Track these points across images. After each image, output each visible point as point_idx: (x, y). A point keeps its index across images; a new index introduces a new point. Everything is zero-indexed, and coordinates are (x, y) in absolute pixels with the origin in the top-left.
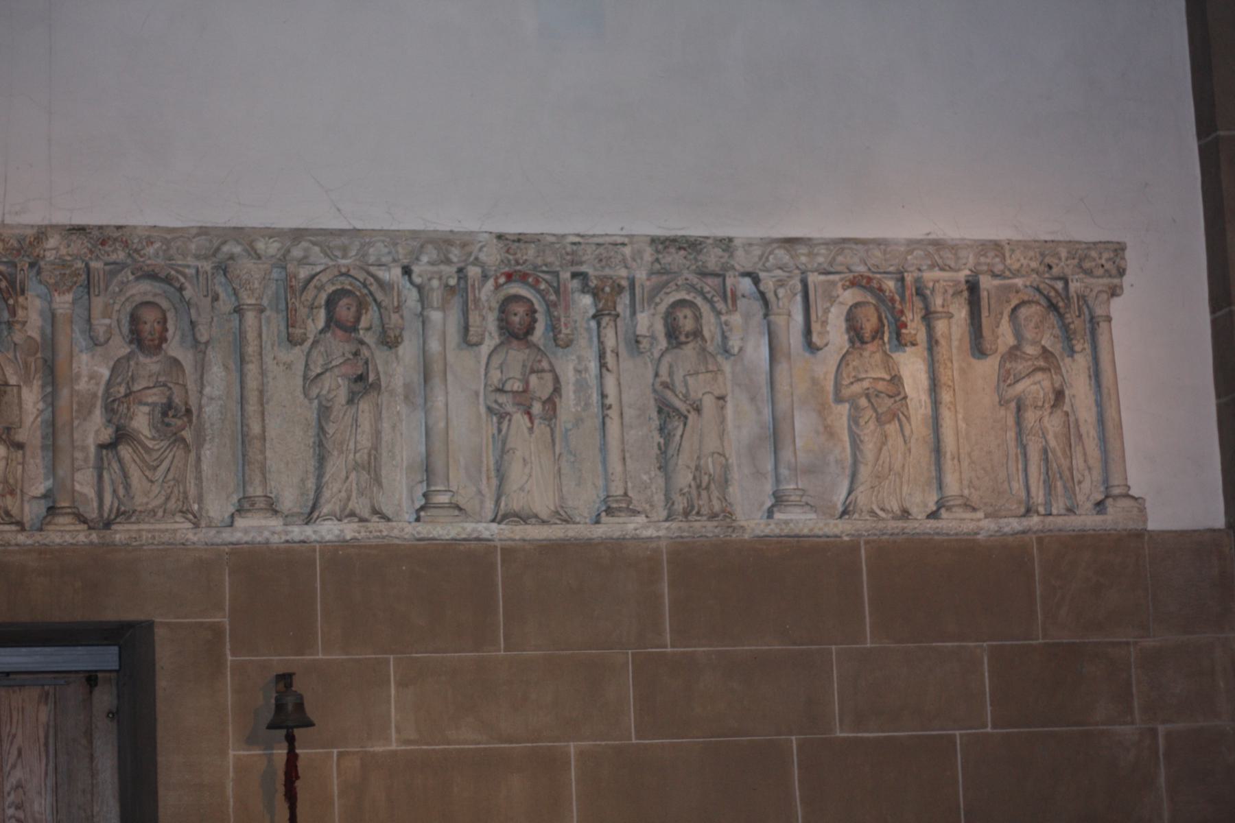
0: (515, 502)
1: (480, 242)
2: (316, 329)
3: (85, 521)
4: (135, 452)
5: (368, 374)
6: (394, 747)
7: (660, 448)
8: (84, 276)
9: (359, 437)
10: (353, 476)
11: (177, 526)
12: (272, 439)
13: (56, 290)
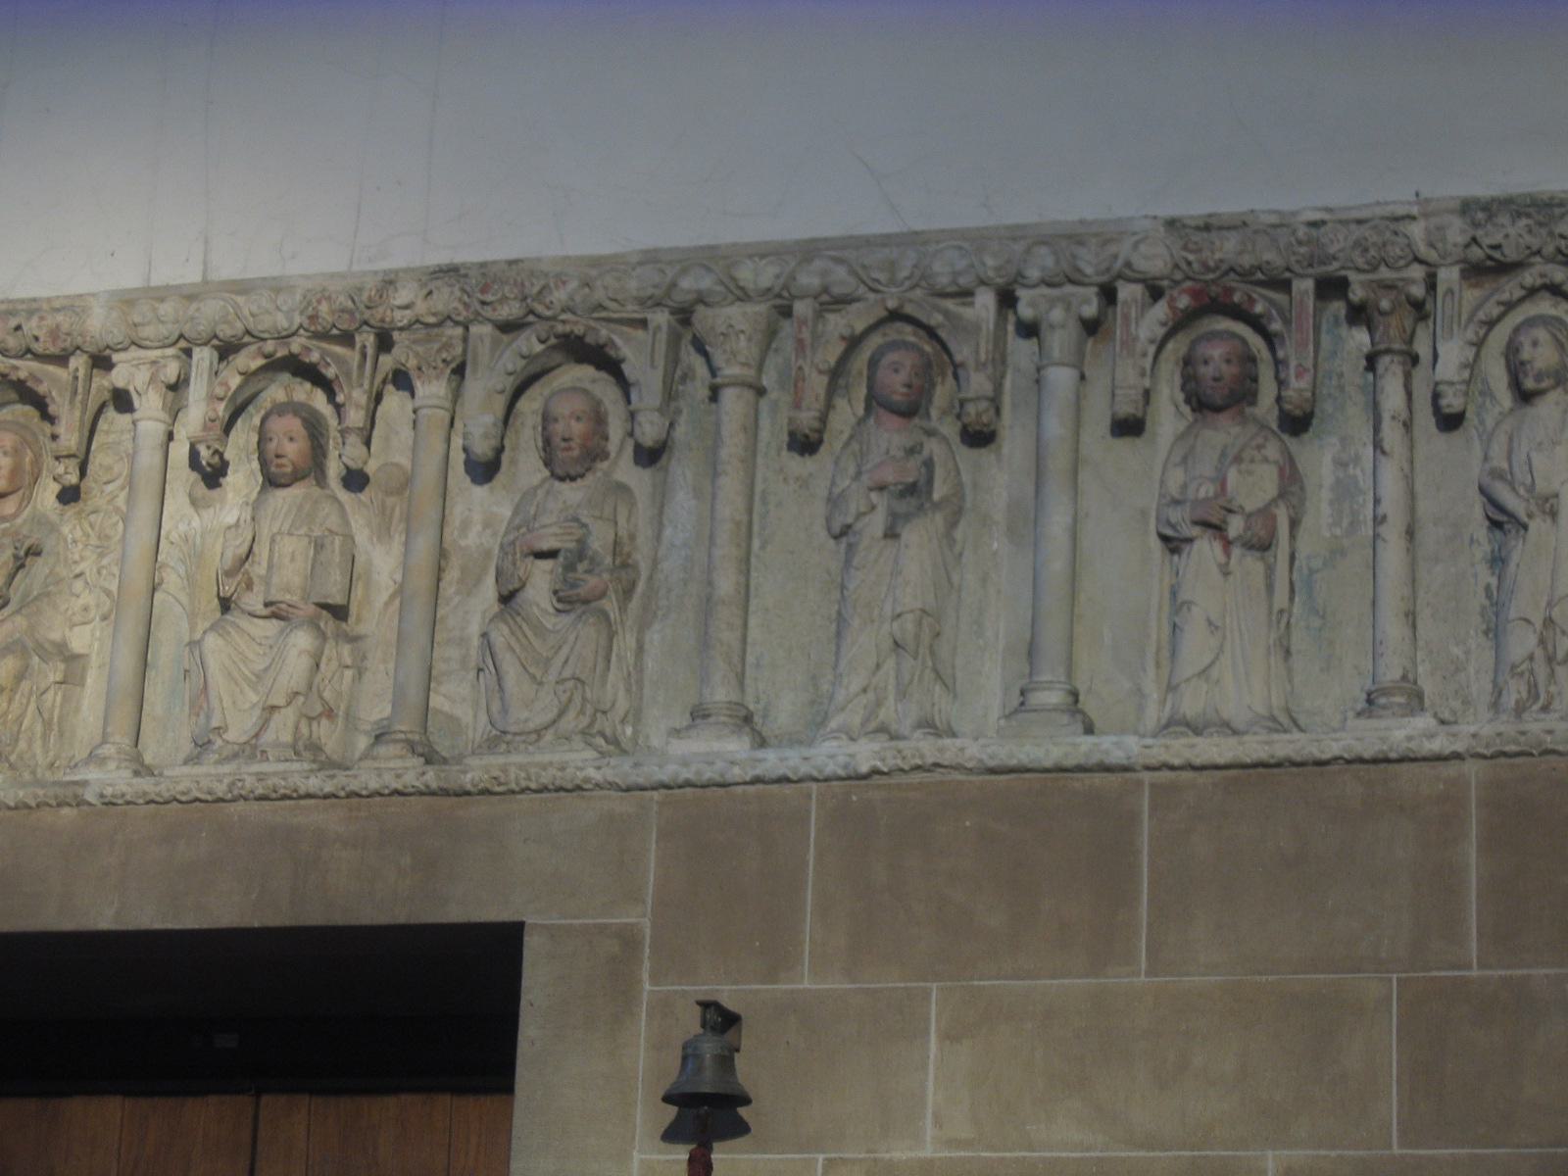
0: (1192, 704)
1: (1134, 234)
4: (513, 633)
6: (927, 1152)
7: (1489, 596)
8: (459, 350)
10: (890, 664)
13: (419, 377)
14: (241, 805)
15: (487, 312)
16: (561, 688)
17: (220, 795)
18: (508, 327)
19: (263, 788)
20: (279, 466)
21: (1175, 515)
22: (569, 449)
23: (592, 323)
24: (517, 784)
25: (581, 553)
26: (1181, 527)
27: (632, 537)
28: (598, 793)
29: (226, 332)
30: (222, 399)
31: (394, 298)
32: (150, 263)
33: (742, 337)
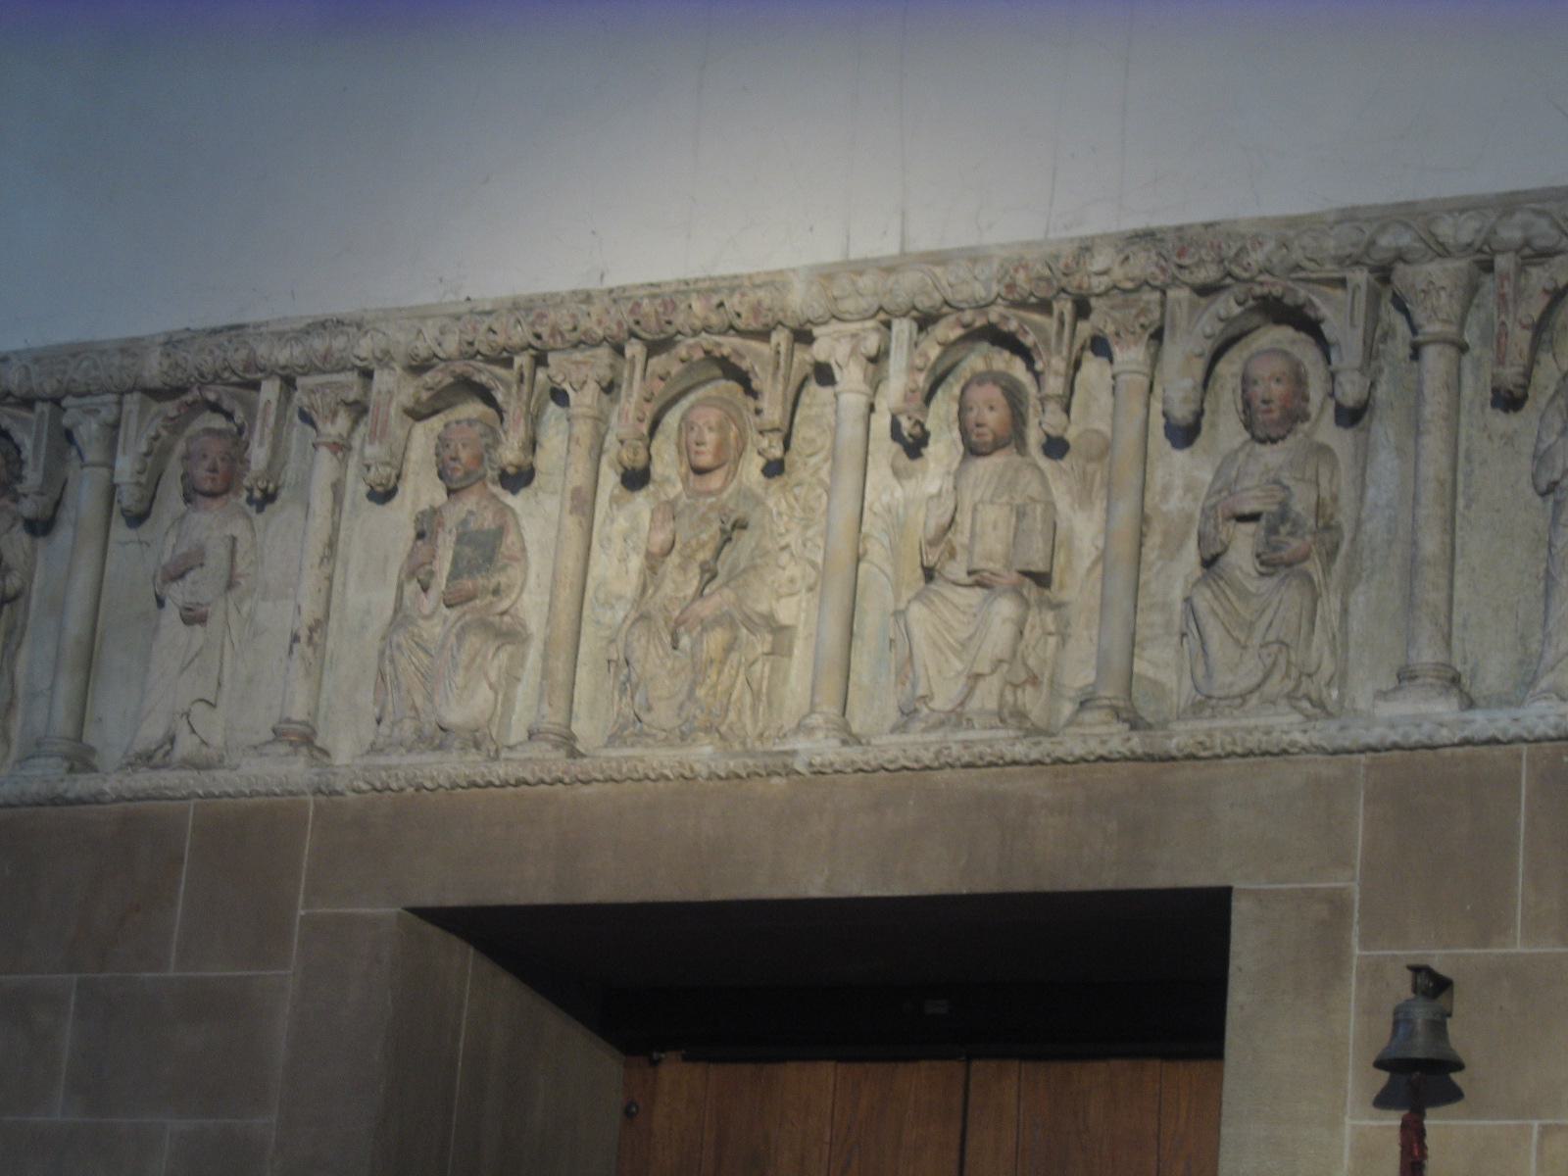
4: (1216, 597)
8: (1157, 314)
13: (1117, 343)
15: (1186, 276)
16: (1265, 651)
17: (927, 763)
18: (1206, 291)
20: (978, 435)
22: (1269, 411)
23: (1290, 284)
25: (1283, 515)
27: (1335, 499)
28: (1304, 757)
29: (924, 303)
30: (920, 370)
31: (1091, 265)
32: (848, 238)
33: (1443, 294)
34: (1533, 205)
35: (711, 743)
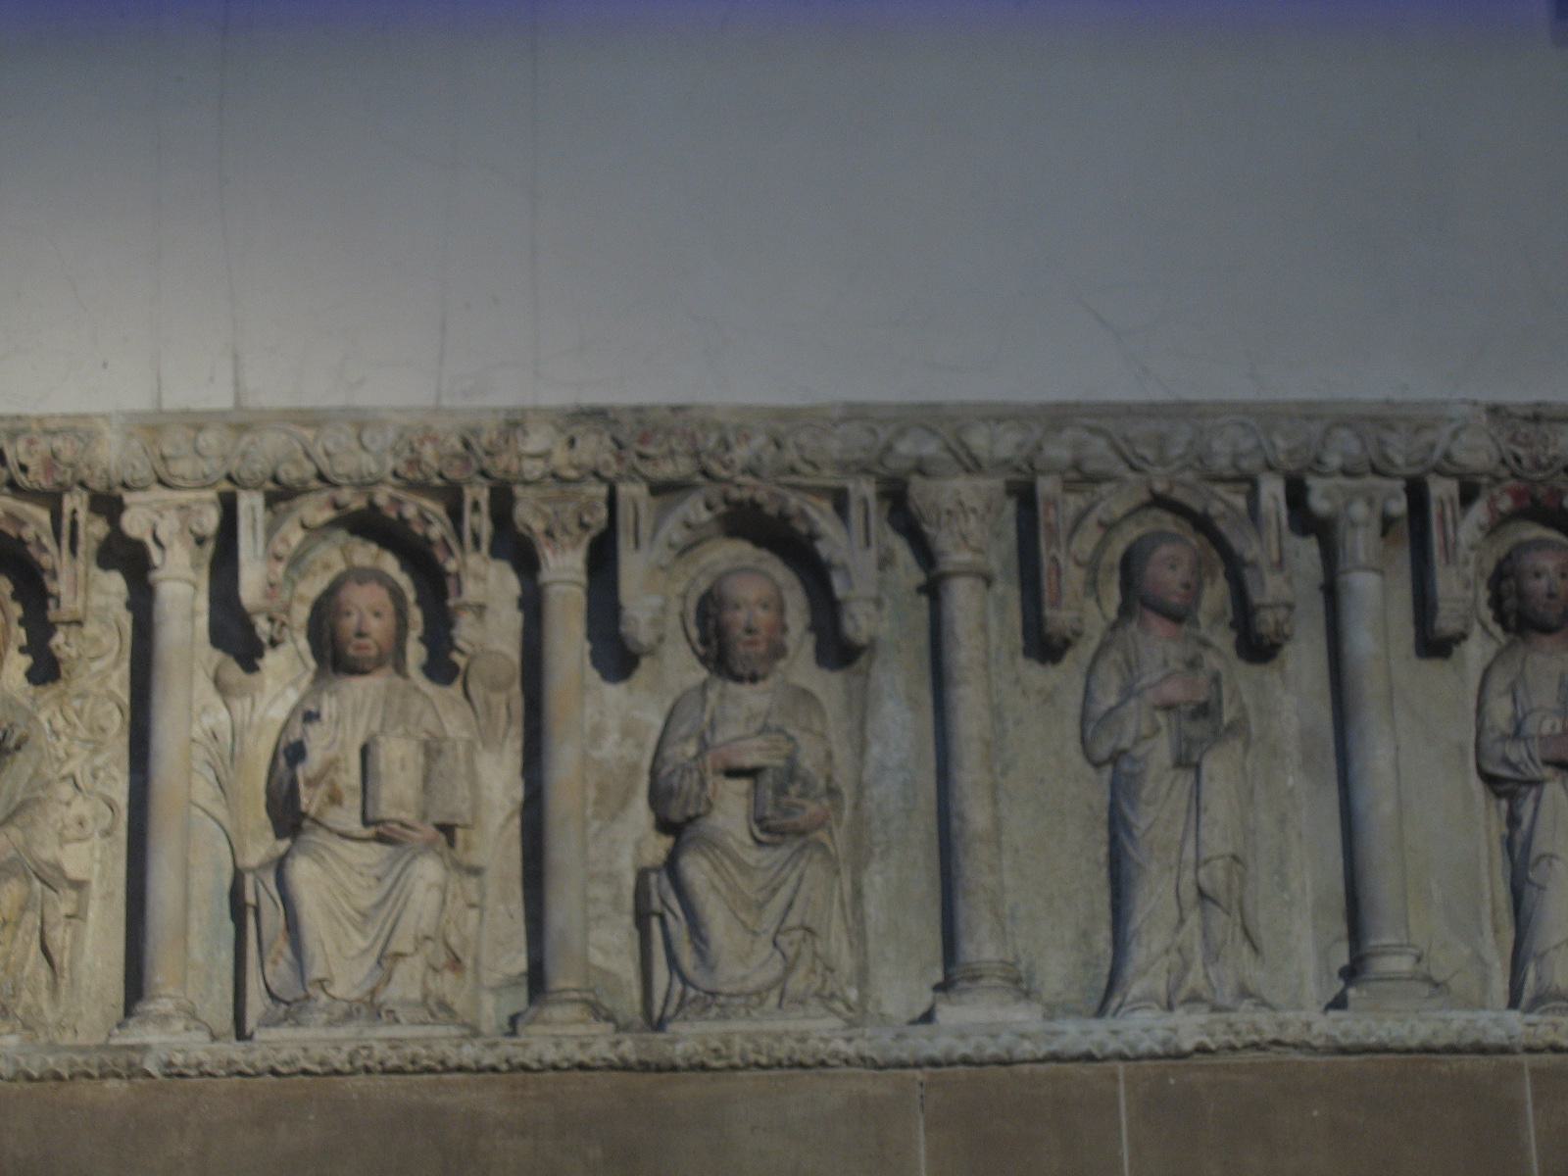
1: (1451, 420)
2: (1104, 617)
3: (609, 1018)
4: (716, 870)
5: (1220, 702)
8: (603, 514)
9: (1204, 833)
11: (808, 1025)
12: (1017, 851)
13: (548, 545)
14: (361, 1080)
15: (647, 469)
17: (338, 1065)
18: (665, 490)
19: (399, 1057)
20: (359, 648)
21: (1516, 752)
23: (778, 490)
24: (742, 1059)
25: (791, 772)
26: (1526, 766)
28: (845, 1070)
29: (290, 473)
30: (278, 558)
32: (159, 380)
34: (1087, 421)
35: (12, 1032)
